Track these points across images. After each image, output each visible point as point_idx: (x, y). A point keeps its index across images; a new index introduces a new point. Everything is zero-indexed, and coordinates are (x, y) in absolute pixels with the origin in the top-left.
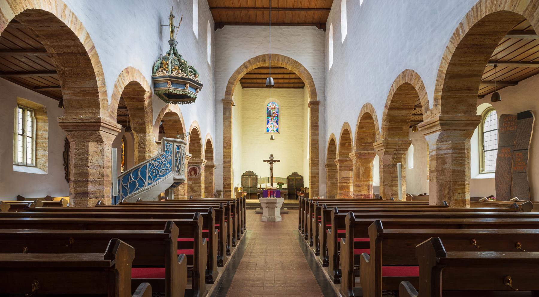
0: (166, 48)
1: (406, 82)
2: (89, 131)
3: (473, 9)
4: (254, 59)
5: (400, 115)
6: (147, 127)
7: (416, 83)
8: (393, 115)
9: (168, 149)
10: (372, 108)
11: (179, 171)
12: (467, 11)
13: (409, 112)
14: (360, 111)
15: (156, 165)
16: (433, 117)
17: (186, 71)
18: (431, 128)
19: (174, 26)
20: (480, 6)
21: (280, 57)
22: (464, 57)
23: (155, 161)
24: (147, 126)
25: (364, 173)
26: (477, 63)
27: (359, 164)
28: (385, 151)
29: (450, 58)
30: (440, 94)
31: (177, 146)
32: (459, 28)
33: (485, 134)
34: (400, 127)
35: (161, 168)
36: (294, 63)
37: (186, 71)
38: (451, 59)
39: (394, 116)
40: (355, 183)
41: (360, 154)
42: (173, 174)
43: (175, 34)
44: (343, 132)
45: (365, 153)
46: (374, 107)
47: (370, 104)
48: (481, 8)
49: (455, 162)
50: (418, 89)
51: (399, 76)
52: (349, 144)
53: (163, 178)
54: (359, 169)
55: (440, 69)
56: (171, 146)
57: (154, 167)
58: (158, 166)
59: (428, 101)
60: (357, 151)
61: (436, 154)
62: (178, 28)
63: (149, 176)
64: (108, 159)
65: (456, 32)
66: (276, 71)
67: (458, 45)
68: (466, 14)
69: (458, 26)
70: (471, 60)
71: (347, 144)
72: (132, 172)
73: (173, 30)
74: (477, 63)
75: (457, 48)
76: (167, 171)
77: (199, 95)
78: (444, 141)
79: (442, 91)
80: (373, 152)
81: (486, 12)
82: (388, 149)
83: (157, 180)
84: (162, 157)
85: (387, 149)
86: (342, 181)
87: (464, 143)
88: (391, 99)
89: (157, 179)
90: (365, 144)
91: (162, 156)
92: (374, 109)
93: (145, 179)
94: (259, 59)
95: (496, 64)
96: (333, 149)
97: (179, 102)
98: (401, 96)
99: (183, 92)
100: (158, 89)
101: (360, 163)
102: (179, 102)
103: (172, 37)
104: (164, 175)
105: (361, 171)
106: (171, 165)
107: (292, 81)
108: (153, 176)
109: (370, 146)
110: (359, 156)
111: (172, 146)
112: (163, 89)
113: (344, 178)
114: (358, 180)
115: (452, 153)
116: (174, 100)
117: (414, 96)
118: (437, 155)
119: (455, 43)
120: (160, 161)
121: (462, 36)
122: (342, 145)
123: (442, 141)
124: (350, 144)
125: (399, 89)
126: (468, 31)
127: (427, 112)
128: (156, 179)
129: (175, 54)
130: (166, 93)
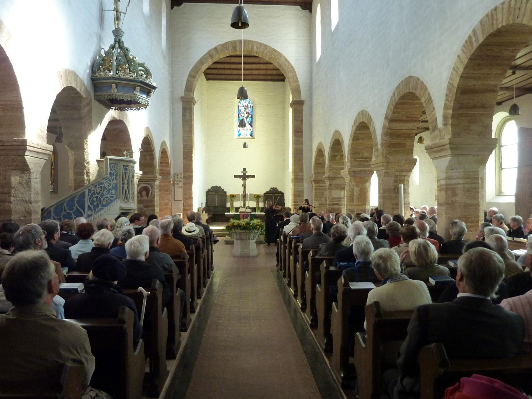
0: (109, 40)
1: (410, 91)
2: (12, 157)
3: (487, 15)
4: (222, 46)
5: (404, 128)
7: (422, 94)
8: (395, 129)
10: (369, 118)
11: (126, 198)
12: (481, 17)
13: (414, 125)
14: (354, 118)
15: (98, 192)
16: (442, 139)
17: (135, 71)
18: (439, 151)
19: (120, 12)
20: (496, 14)
21: (255, 44)
22: (478, 70)
23: (96, 186)
25: (359, 195)
26: (493, 77)
27: (353, 183)
28: (386, 173)
29: (462, 69)
30: (450, 111)
31: (124, 166)
32: (472, 35)
33: (502, 148)
34: (403, 142)
36: (272, 52)
37: (135, 71)
38: (463, 71)
39: (396, 130)
40: (348, 207)
41: (354, 172)
42: (120, 203)
43: (121, 23)
44: (333, 142)
45: (361, 171)
46: (372, 117)
47: (367, 111)
48: (496, 15)
49: (467, 194)
50: (425, 103)
51: (402, 82)
52: (340, 157)
53: (106, 208)
54: (353, 190)
55: (450, 81)
56: (116, 167)
57: (95, 195)
58: (100, 192)
59: (436, 118)
60: (351, 169)
61: (445, 183)
62: (125, 14)
63: (89, 206)
64: (37, 190)
65: (469, 40)
66: (250, 60)
67: (471, 56)
68: (479, 20)
69: (470, 32)
70: (486, 73)
71: (338, 157)
72: (66, 202)
73: (118, 17)
74: (493, 77)
75: (469, 59)
76: (112, 199)
77: (152, 99)
78: (455, 168)
79: (452, 108)
80: (370, 169)
81: (502, 21)
82: (388, 170)
83: (98, 211)
84: (105, 182)
85: (387, 169)
86: (332, 203)
87: (478, 171)
88: (393, 109)
89: (98, 209)
90: (360, 160)
91: (105, 180)
92: (371, 119)
93: (84, 210)
94: (227, 45)
95: (514, 70)
96: (321, 161)
97: (126, 108)
98: (403, 106)
99: (131, 97)
100: (99, 94)
101: (355, 183)
102: (126, 108)
103: (117, 26)
104: (108, 204)
105: (355, 193)
106: (116, 190)
107: (270, 72)
109: (367, 161)
110: (353, 174)
112: (105, 94)
113: (334, 198)
114: (352, 204)
115: (464, 184)
116: (119, 106)
117: (419, 107)
118: (447, 185)
119: (467, 53)
120: (102, 187)
121: (475, 45)
122: (333, 157)
123: (452, 168)
124: (342, 156)
125: (403, 98)
126: (482, 42)
127: (435, 131)
128: (97, 210)
129: (121, 47)
130: (110, 98)
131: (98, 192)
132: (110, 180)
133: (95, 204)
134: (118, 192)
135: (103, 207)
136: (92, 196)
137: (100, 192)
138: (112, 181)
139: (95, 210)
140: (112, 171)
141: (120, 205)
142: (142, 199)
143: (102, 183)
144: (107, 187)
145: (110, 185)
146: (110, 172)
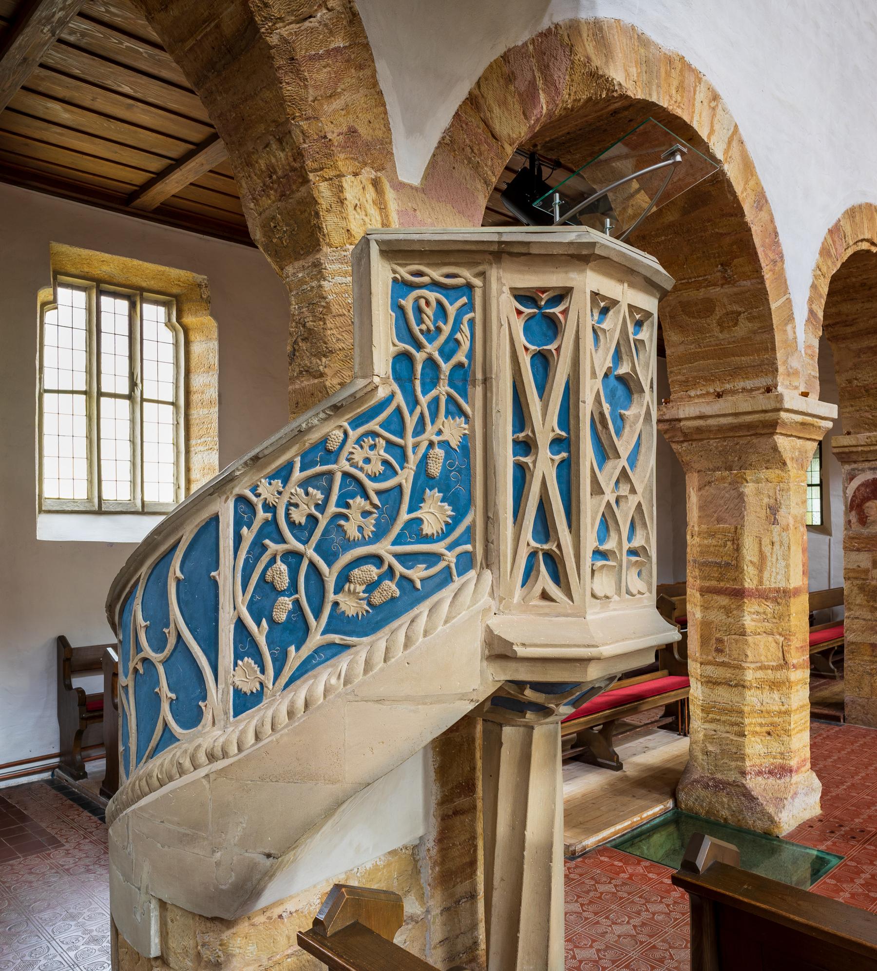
6: (324, 192)
9: (419, 346)
15: (299, 517)
24: (324, 187)
31: (525, 297)
35: (350, 544)
58: (313, 520)
63: (240, 624)
76: (418, 573)
84: (353, 435)
91: (356, 423)
93: (211, 647)
108: (272, 622)
111: (473, 309)
120: (330, 474)
128: (295, 657)
131: (299, 517)
132: (397, 423)
133: (283, 607)
134: (474, 516)
135: (336, 638)
136: (259, 547)
137: (313, 520)
138: (416, 433)
139: (280, 662)
140: (419, 346)
141: (494, 622)
142: (865, 531)
143: (333, 446)
144: (374, 478)
145: (403, 458)
146: (403, 360)
